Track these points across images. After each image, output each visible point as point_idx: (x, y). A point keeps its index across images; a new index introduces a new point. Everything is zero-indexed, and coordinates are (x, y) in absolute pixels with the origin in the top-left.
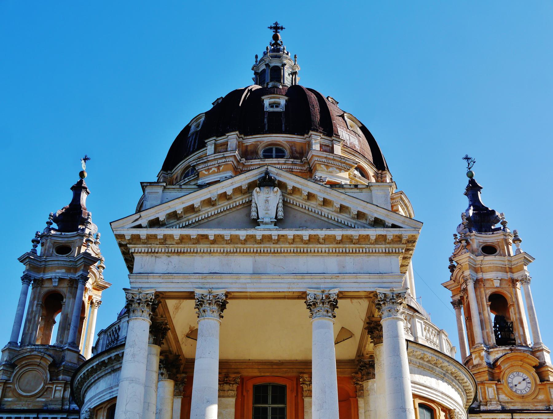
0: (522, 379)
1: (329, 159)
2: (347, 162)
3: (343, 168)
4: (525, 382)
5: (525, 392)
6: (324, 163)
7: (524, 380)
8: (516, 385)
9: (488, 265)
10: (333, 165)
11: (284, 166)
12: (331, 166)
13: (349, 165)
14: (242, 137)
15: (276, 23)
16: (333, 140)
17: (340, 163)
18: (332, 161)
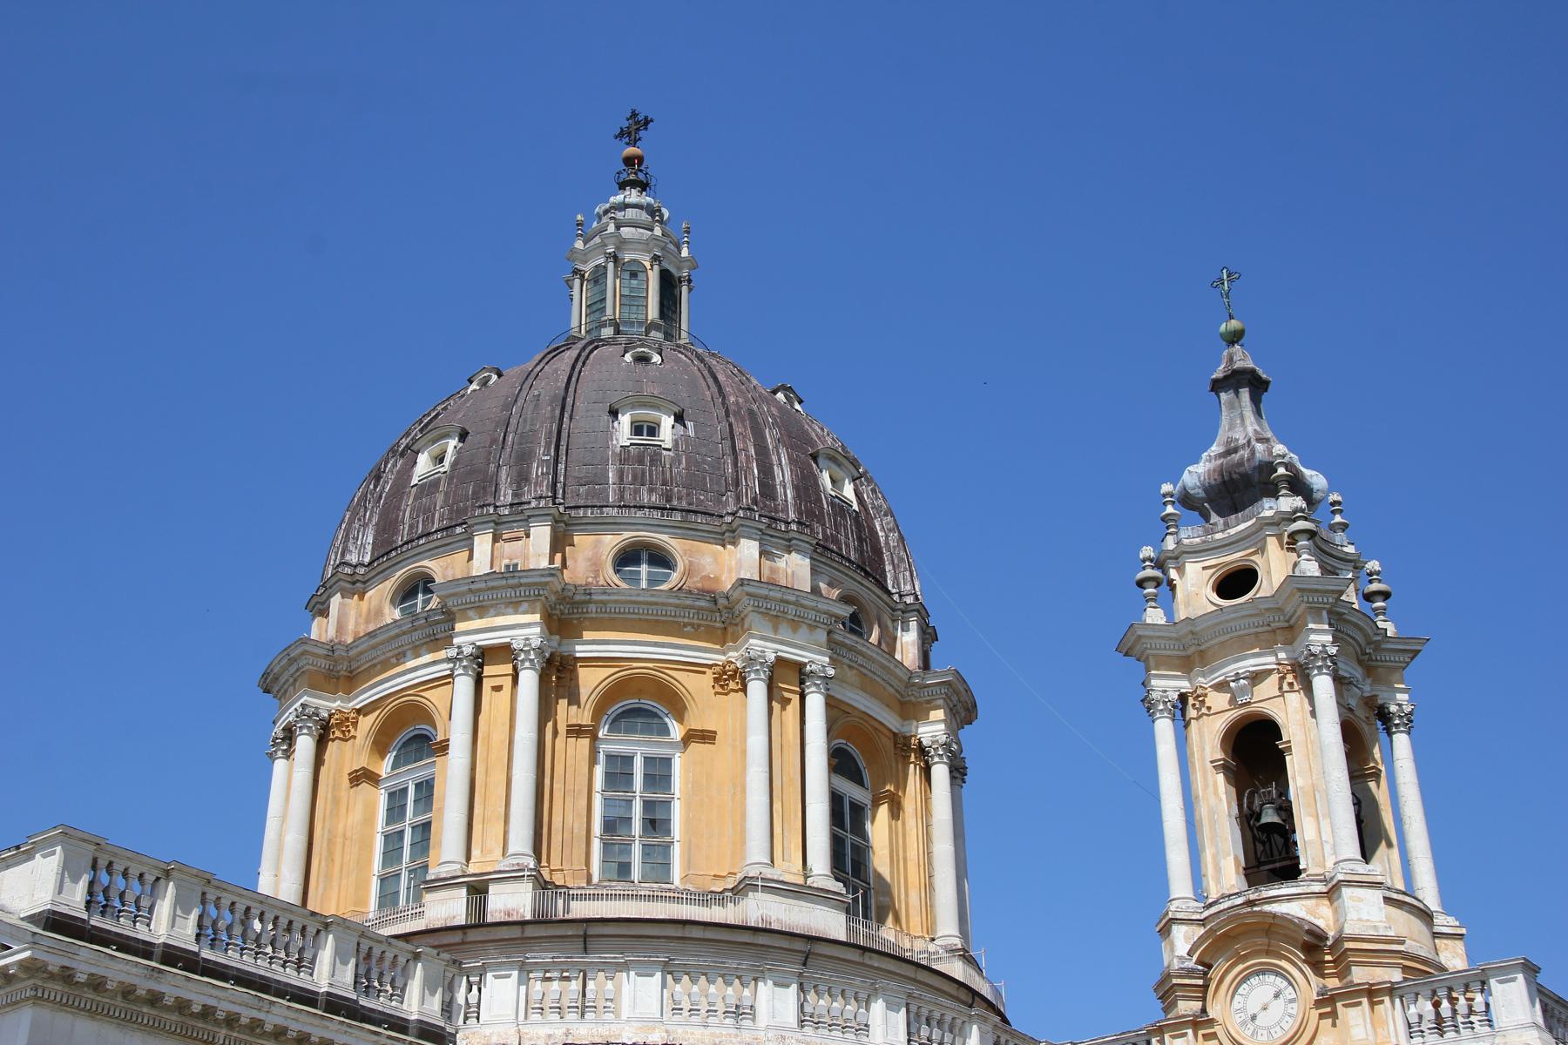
0: (1272, 991)
1: (479, 590)
2: (522, 581)
3: (522, 599)
4: (1281, 999)
5: (1280, 1033)
6: (473, 605)
7: (1277, 996)
8: (1254, 1018)
9: (1216, 641)
10: (494, 602)
11: (416, 635)
12: (492, 606)
13: (535, 584)
14: (358, 581)
15: (634, 114)
16: (529, 517)
17: (510, 590)
18: (489, 592)
